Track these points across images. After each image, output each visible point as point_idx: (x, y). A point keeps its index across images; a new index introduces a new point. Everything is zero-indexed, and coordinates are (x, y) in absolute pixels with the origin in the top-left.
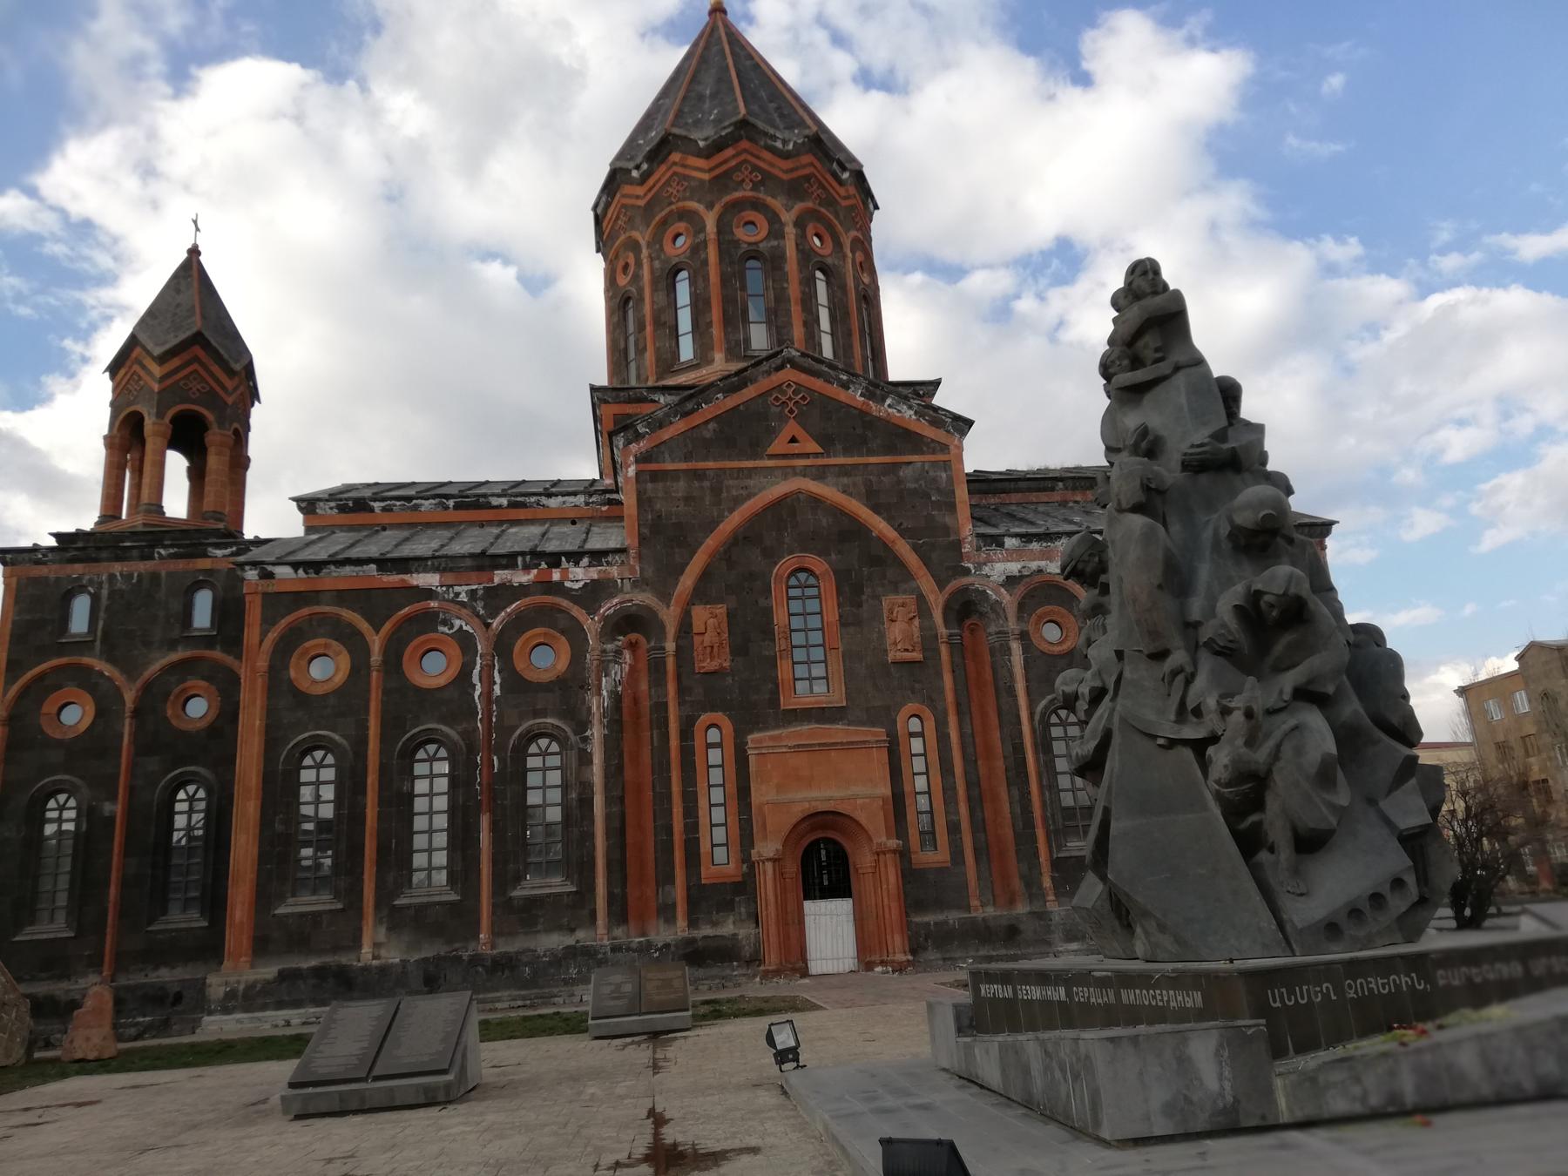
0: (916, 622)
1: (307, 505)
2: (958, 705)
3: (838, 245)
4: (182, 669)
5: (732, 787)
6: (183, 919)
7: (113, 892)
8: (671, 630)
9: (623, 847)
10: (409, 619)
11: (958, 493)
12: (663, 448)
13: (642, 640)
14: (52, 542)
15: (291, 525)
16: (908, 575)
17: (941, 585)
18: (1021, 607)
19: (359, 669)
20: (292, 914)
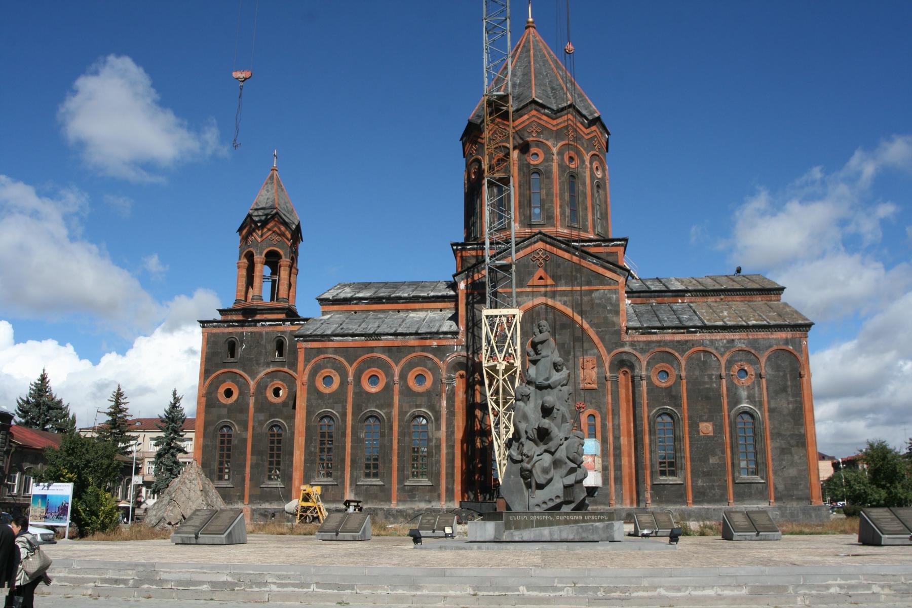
2: (613, 410)
10: (363, 361)
17: (609, 352)
18: (648, 363)
19: (344, 383)
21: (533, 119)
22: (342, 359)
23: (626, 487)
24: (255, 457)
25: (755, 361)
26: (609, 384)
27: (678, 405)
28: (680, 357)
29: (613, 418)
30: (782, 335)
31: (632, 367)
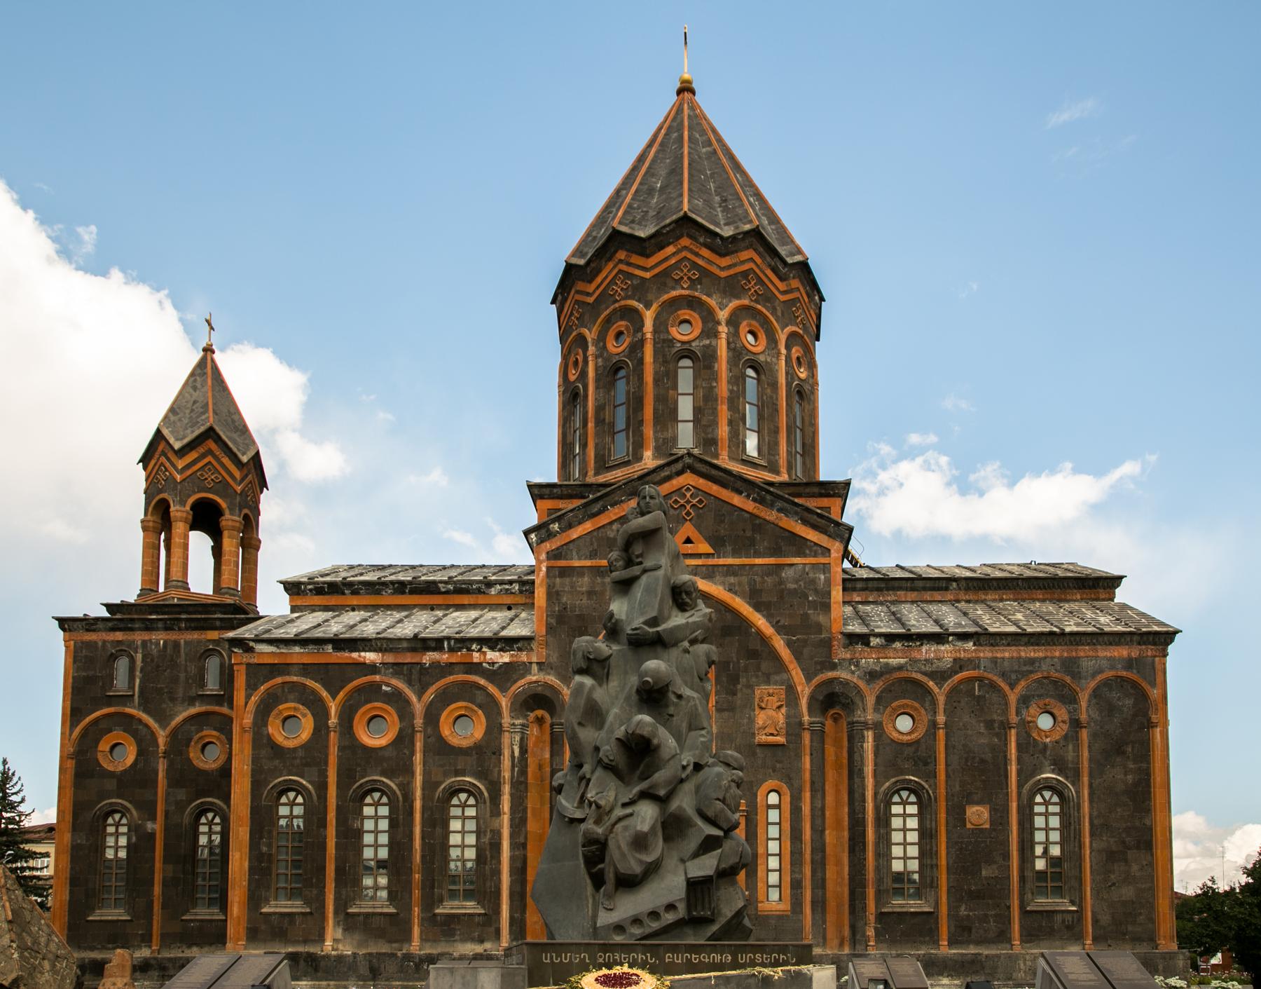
2: (813, 783)
10: (358, 690)
11: (833, 593)
13: (547, 716)
17: (809, 678)
18: (879, 699)
20: (275, 913)
21: (684, 254)
23: (830, 918)
25: (1069, 698)
26: (806, 737)
28: (936, 689)
29: (812, 797)
30: (1122, 652)
31: (849, 706)
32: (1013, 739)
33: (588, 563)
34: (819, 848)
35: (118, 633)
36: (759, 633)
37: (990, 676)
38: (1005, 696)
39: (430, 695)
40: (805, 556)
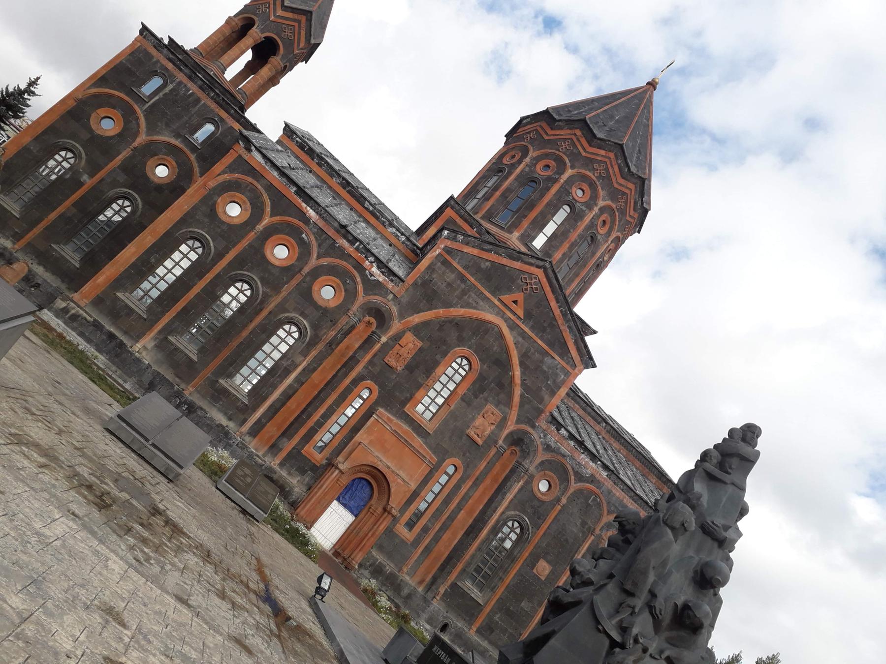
0: (493, 427)
1: (289, 131)
3: (609, 233)
4: (172, 150)
5: (353, 423)
6: (71, 254)
7: (53, 216)
8: (391, 333)
9: (284, 404)
10: (289, 224)
11: (562, 389)
12: (460, 253)
14: (166, 41)
15: (273, 132)
16: (509, 403)
17: (518, 421)
18: (542, 463)
22: (268, 202)
24: (74, 210)
26: (493, 451)
27: (537, 527)
28: (573, 481)
31: (525, 454)
32: (590, 542)
33: (460, 269)
34: (452, 518)
35: (170, 64)
36: (512, 378)
37: (603, 498)
38: (601, 515)
39: (325, 261)
40: (563, 359)
